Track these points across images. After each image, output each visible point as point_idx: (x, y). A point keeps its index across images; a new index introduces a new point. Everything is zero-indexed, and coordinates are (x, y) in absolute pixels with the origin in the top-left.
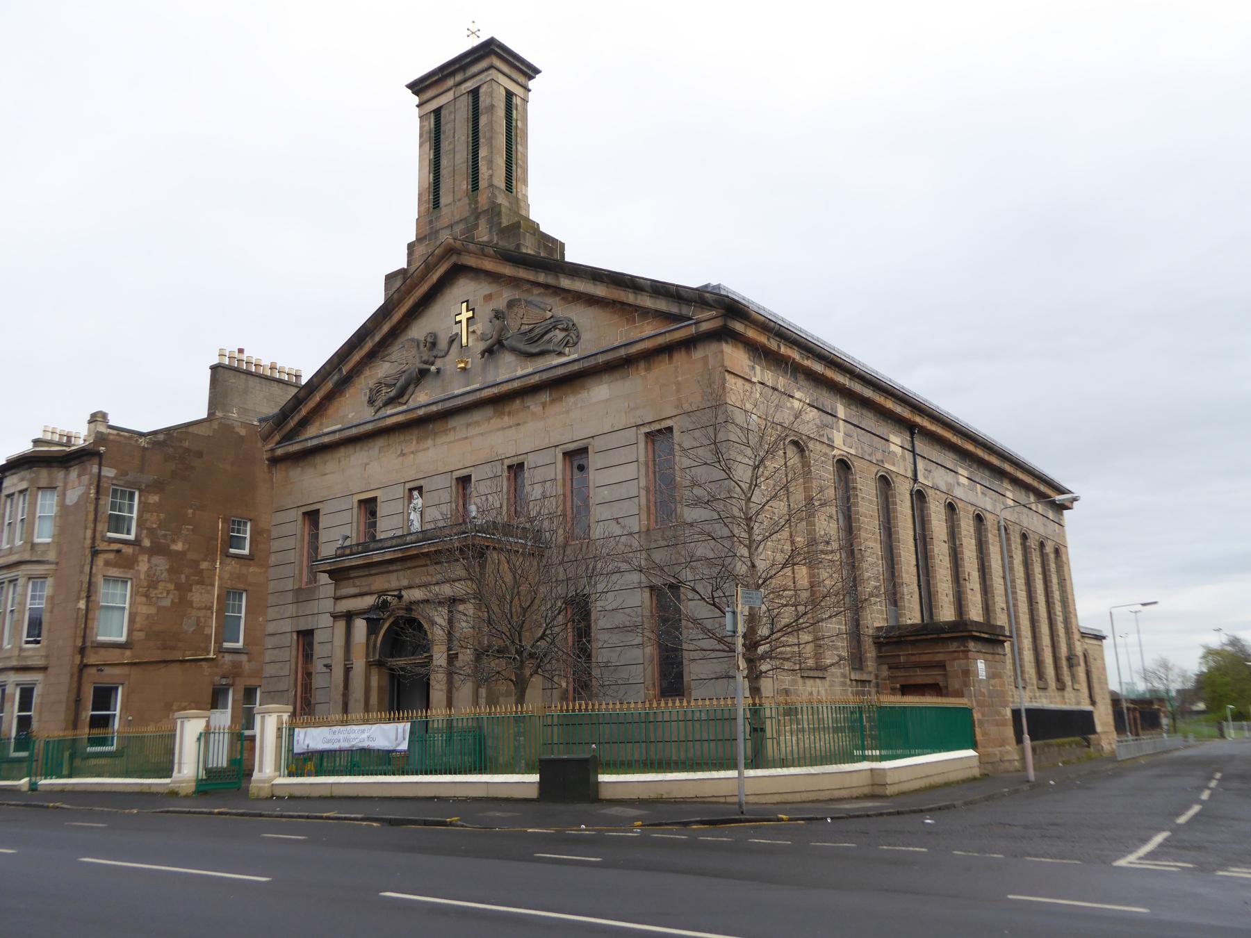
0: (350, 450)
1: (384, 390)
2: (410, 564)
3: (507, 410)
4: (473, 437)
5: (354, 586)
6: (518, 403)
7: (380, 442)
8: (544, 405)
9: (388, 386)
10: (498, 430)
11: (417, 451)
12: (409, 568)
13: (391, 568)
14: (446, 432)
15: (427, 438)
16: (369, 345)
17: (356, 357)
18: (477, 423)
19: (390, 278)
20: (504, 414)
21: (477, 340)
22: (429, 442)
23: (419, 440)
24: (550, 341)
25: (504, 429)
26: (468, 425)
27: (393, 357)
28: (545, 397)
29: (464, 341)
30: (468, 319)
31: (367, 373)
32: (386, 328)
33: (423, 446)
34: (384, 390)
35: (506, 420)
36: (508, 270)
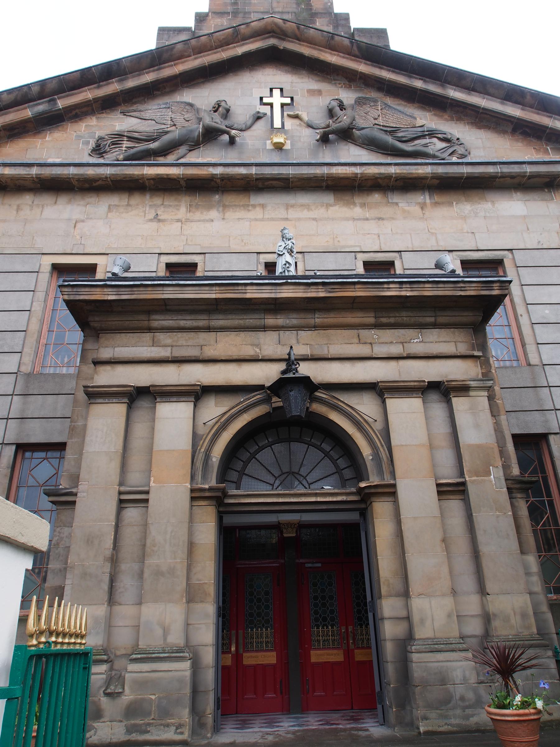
0: (46, 199)
1: (126, 144)
2: (319, 319)
3: (358, 200)
4: (299, 219)
5: (154, 343)
6: (376, 197)
7: (114, 199)
8: (423, 206)
9: (130, 139)
10: (347, 219)
11: (187, 220)
12: (315, 327)
13: (270, 321)
14: (246, 207)
15: (210, 207)
16: (113, 87)
17: (87, 94)
18: (307, 207)
19: (163, 31)
20: (354, 204)
21: (300, 125)
22: (214, 214)
23: (190, 208)
24: (426, 145)
25: (354, 219)
26: (288, 207)
27: (147, 115)
28: (424, 198)
29: (277, 123)
30: (283, 105)
31: (92, 121)
32: (148, 77)
33: (198, 215)
34: (126, 144)
35: (357, 211)
36: (363, 68)
